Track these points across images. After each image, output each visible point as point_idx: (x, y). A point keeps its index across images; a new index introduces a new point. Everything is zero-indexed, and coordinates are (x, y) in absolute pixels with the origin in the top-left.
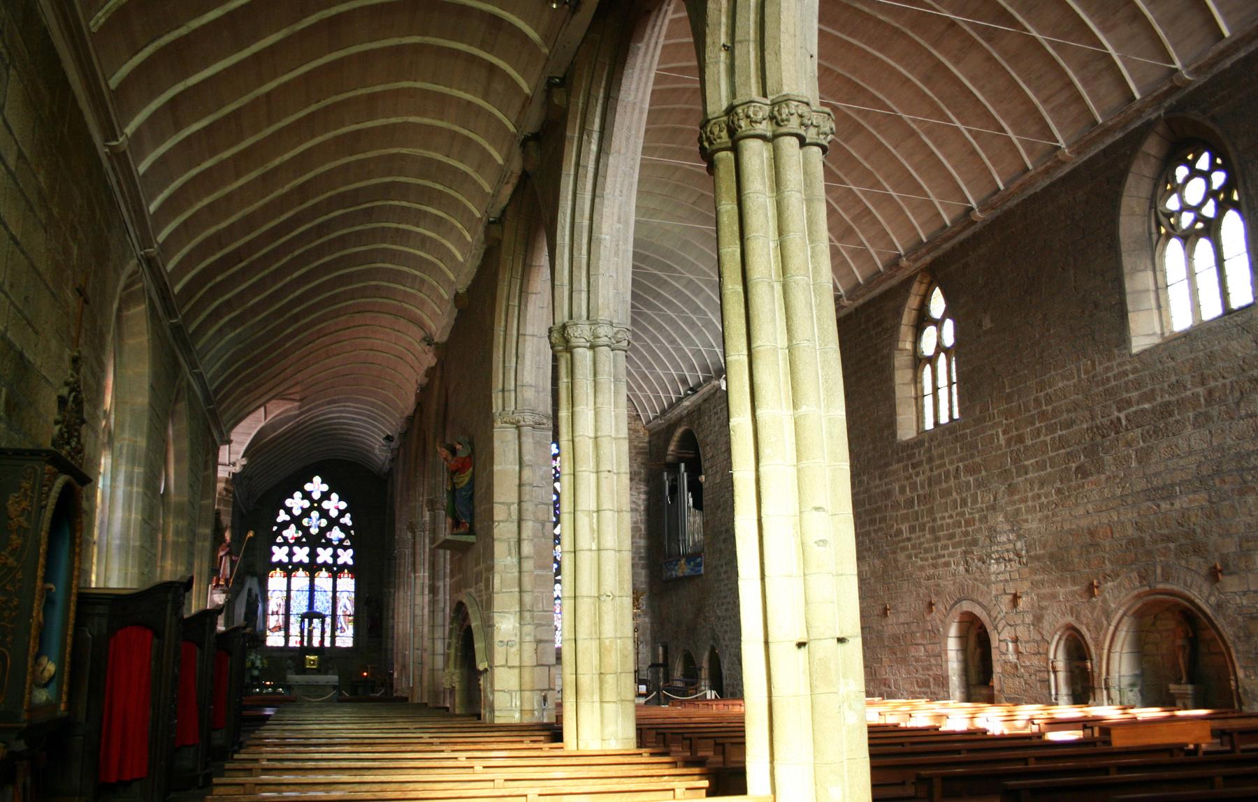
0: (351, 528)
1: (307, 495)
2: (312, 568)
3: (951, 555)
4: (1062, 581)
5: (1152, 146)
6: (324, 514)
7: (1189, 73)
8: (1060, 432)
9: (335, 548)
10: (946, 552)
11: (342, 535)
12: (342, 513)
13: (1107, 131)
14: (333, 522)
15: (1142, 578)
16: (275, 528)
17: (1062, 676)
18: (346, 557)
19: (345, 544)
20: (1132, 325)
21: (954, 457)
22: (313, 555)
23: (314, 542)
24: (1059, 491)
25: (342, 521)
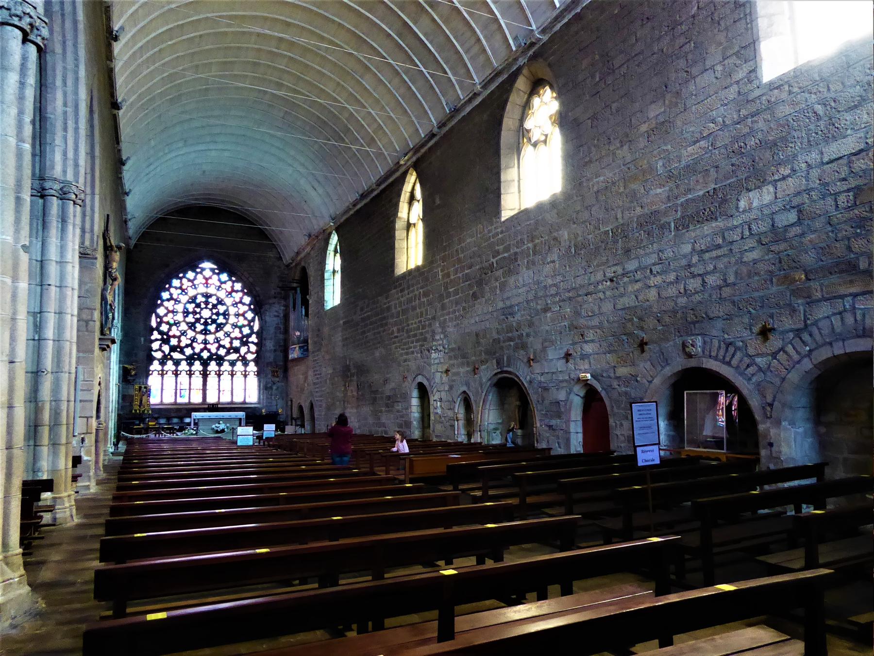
3: (415, 347)
4: (462, 364)
5: (522, 84)
7: (539, 33)
8: (466, 271)
10: (412, 345)
13: (498, 74)
15: (498, 363)
20: (502, 202)
21: (419, 286)
24: (464, 309)
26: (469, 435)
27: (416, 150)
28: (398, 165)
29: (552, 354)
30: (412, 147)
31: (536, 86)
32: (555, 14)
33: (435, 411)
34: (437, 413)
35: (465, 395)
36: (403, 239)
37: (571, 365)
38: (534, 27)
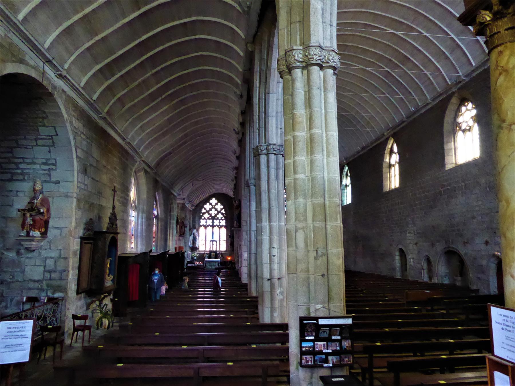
0: (225, 214)
1: (211, 204)
2: (213, 226)
5: (454, 100)
6: (216, 210)
8: (426, 194)
9: (220, 220)
11: (222, 216)
12: (222, 209)
13: (441, 95)
14: (219, 212)
15: (446, 242)
16: (201, 214)
17: (426, 271)
18: (223, 223)
19: (223, 219)
20: (446, 161)
22: (213, 222)
23: (213, 218)
24: (425, 213)
25: (222, 212)
26: (430, 278)
27: (394, 128)
28: (383, 135)
29: (477, 240)
30: (391, 126)
31: (463, 102)
32: (472, 69)
33: (410, 264)
34: (411, 265)
35: (427, 257)
36: (387, 173)
37: (489, 247)
38: (461, 74)
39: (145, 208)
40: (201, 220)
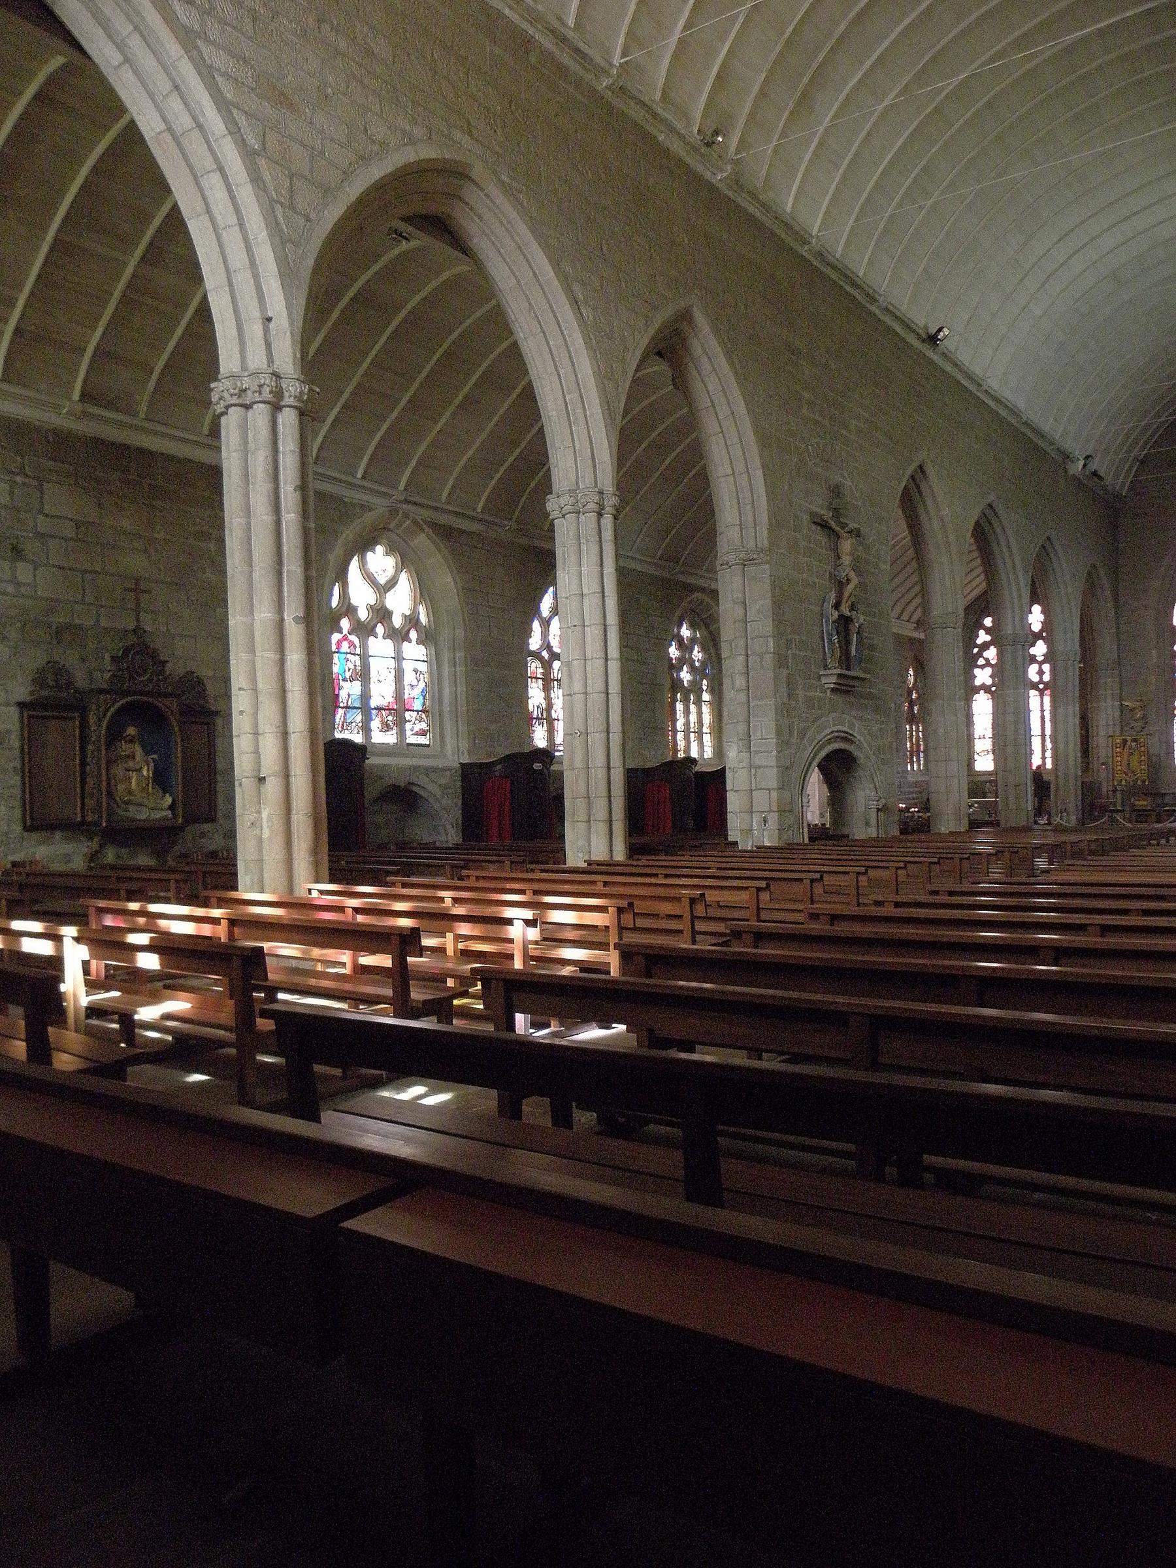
16: (976, 650)
39: (460, 633)
40: (977, 671)
